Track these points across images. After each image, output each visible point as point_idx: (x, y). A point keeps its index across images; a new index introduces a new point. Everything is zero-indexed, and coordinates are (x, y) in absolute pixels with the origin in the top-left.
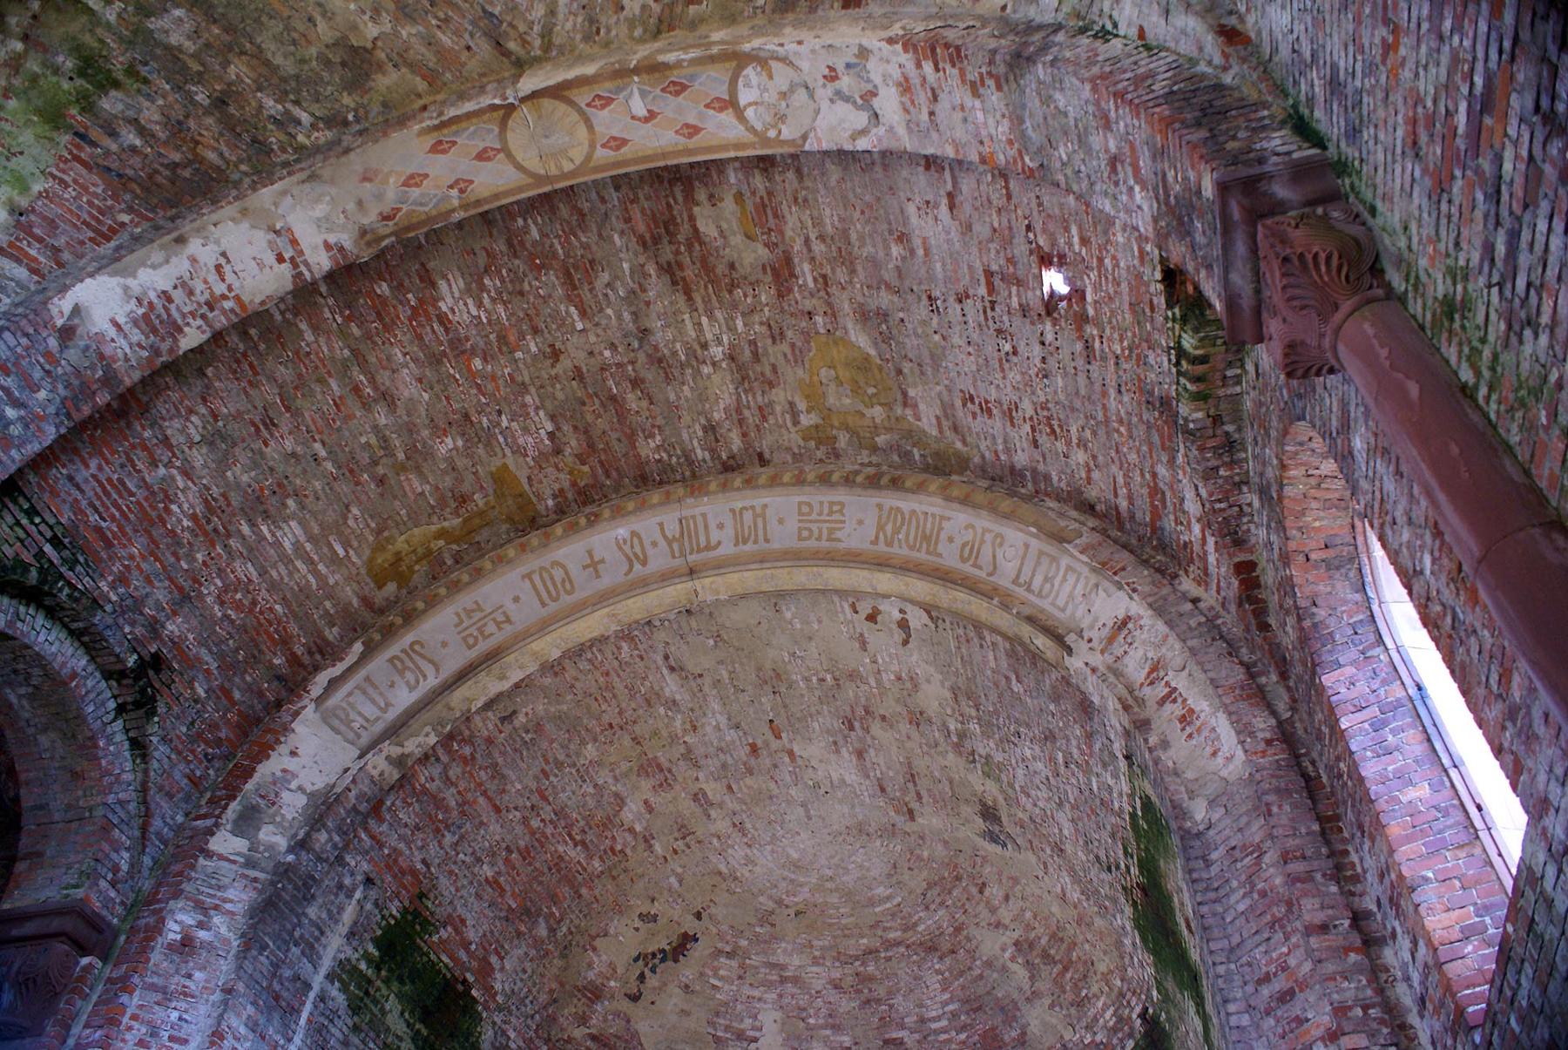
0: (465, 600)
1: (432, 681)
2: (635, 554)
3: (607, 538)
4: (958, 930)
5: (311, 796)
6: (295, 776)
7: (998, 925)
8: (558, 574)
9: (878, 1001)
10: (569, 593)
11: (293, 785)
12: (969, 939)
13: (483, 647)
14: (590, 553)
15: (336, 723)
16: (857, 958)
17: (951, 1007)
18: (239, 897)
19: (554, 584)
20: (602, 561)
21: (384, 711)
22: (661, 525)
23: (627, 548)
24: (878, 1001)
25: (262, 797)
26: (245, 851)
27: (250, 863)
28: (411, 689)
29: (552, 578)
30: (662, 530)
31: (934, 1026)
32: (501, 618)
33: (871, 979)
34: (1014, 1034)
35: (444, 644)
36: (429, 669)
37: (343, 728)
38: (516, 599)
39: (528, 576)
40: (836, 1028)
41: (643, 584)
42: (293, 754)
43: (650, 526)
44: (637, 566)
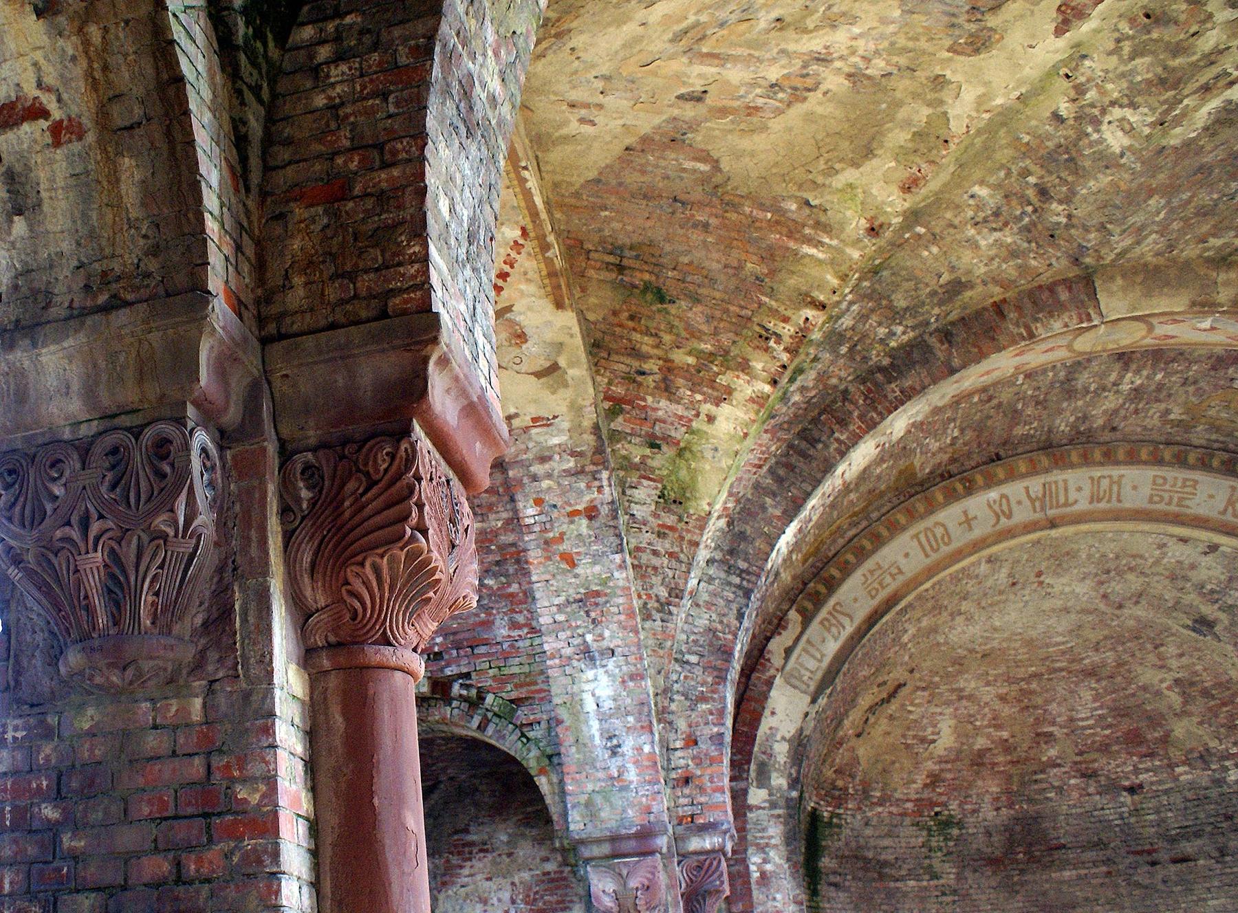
0: (870, 564)
1: (849, 629)
2: (1002, 511)
3: (980, 504)
4: (1120, 665)
5: (789, 741)
6: (777, 729)
7: (1162, 667)
8: (939, 531)
9: (1035, 707)
10: (946, 544)
11: (778, 738)
12: (1129, 671)
13: (883, 595)
14: (965, 513)
15: (793, 681)
16: (1023, 679)
17: (1100, 712)
18: (775, 832)
19: (936, 541)
20: (975, 518)
21: (820, 661)
22: (1027, 489)
23: (996, 507)
24: (1035, 707)
25: (764, 753)
26: (767, 797)
27: (773, 805)
28: (836, 639)
29: (934, 536)
30: (1028, 492)
31: (1081, 724)
32: (894, 571)
33: (1032, 692)
34: (1156, 735)
35: (856, 600)
36: (846, 621)
37: (797, 683)
38: (907, 555)
39: (916, 536)
40: (998, 727)
41: (1009, 534)
42: (773, 713)
43: (1018, 495)
44: (1003, 520)
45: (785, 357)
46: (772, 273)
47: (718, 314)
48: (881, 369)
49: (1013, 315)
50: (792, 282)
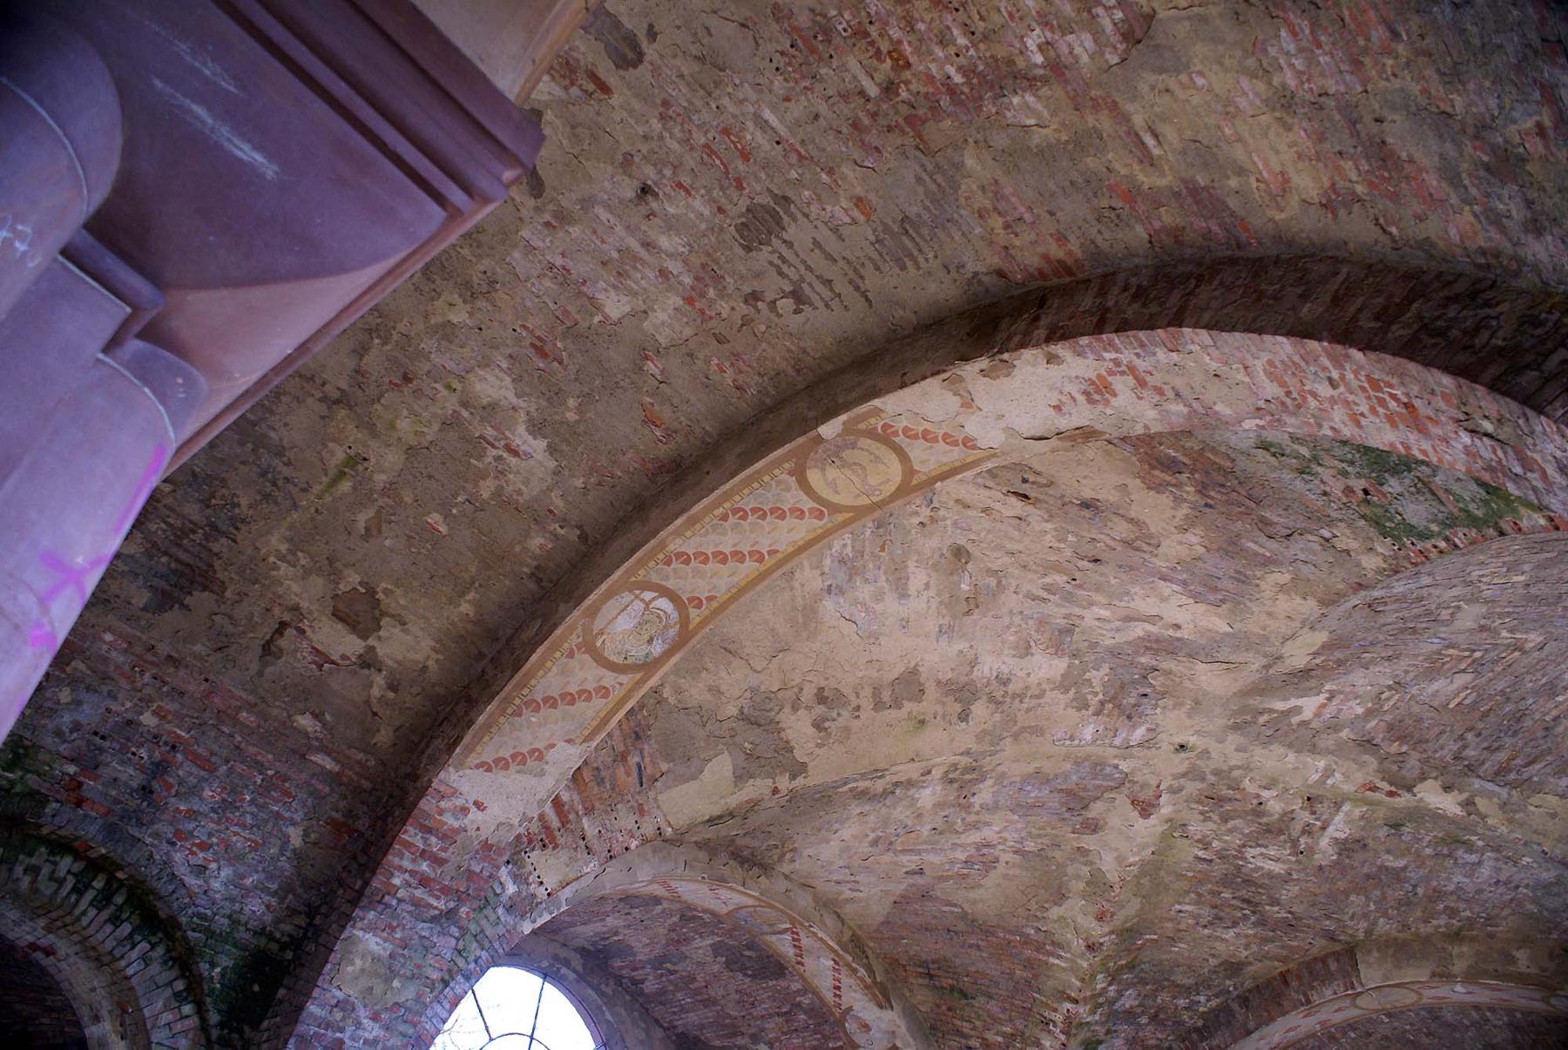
45: (1063, 1037)
46: (1035, 976)
47: (1007, 1006)
48: (1197, 1030)
49: (1294, 984)
50: (1050, 983)
